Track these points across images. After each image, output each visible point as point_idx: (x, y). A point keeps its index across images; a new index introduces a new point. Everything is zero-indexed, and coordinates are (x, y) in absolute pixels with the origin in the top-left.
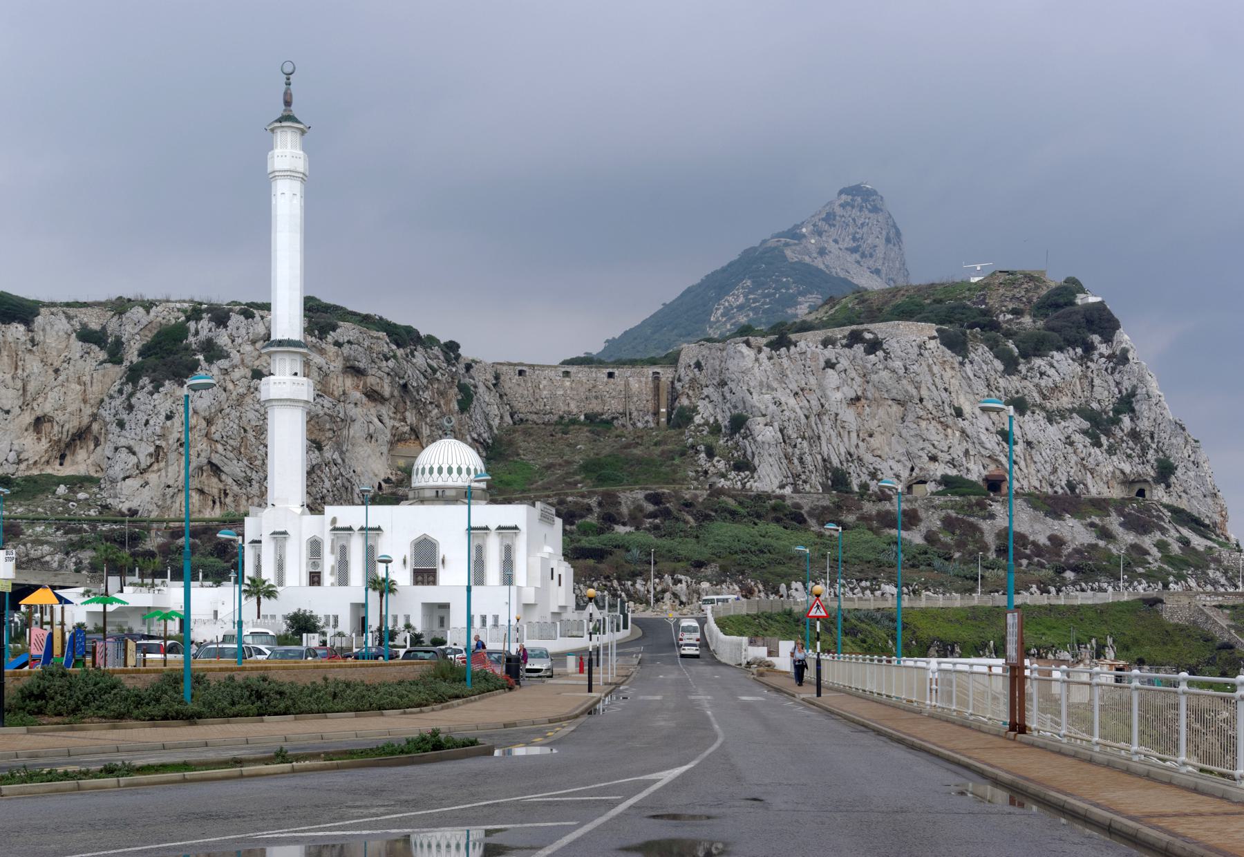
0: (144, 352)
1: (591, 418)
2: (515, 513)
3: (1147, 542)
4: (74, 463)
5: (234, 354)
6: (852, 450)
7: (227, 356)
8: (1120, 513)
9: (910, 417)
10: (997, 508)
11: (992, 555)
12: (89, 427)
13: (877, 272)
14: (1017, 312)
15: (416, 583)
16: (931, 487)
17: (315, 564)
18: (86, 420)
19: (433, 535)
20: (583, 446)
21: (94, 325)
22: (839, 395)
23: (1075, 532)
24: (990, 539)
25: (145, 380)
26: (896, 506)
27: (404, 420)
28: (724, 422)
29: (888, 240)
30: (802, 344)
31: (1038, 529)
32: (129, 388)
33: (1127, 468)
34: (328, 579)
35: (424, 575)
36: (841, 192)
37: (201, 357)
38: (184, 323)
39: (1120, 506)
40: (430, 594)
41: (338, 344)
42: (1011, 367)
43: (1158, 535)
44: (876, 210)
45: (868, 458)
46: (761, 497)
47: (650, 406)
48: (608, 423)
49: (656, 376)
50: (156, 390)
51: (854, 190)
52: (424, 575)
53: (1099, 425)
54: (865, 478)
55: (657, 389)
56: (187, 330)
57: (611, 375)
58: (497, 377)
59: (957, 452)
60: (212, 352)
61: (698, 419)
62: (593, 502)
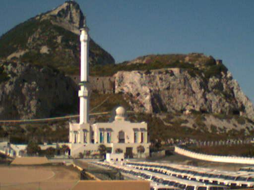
3: (243, 127)
9: (181, 94)
10: (206, 117)
16: (187, 112)
30: (153, 74)
35: (121, 140)
38: (3, 66)
52: (121, 140)
55: (111, 82)
56: (3, 69)
57: (98, 79)
59: (194, 103)
60: (14, 75)
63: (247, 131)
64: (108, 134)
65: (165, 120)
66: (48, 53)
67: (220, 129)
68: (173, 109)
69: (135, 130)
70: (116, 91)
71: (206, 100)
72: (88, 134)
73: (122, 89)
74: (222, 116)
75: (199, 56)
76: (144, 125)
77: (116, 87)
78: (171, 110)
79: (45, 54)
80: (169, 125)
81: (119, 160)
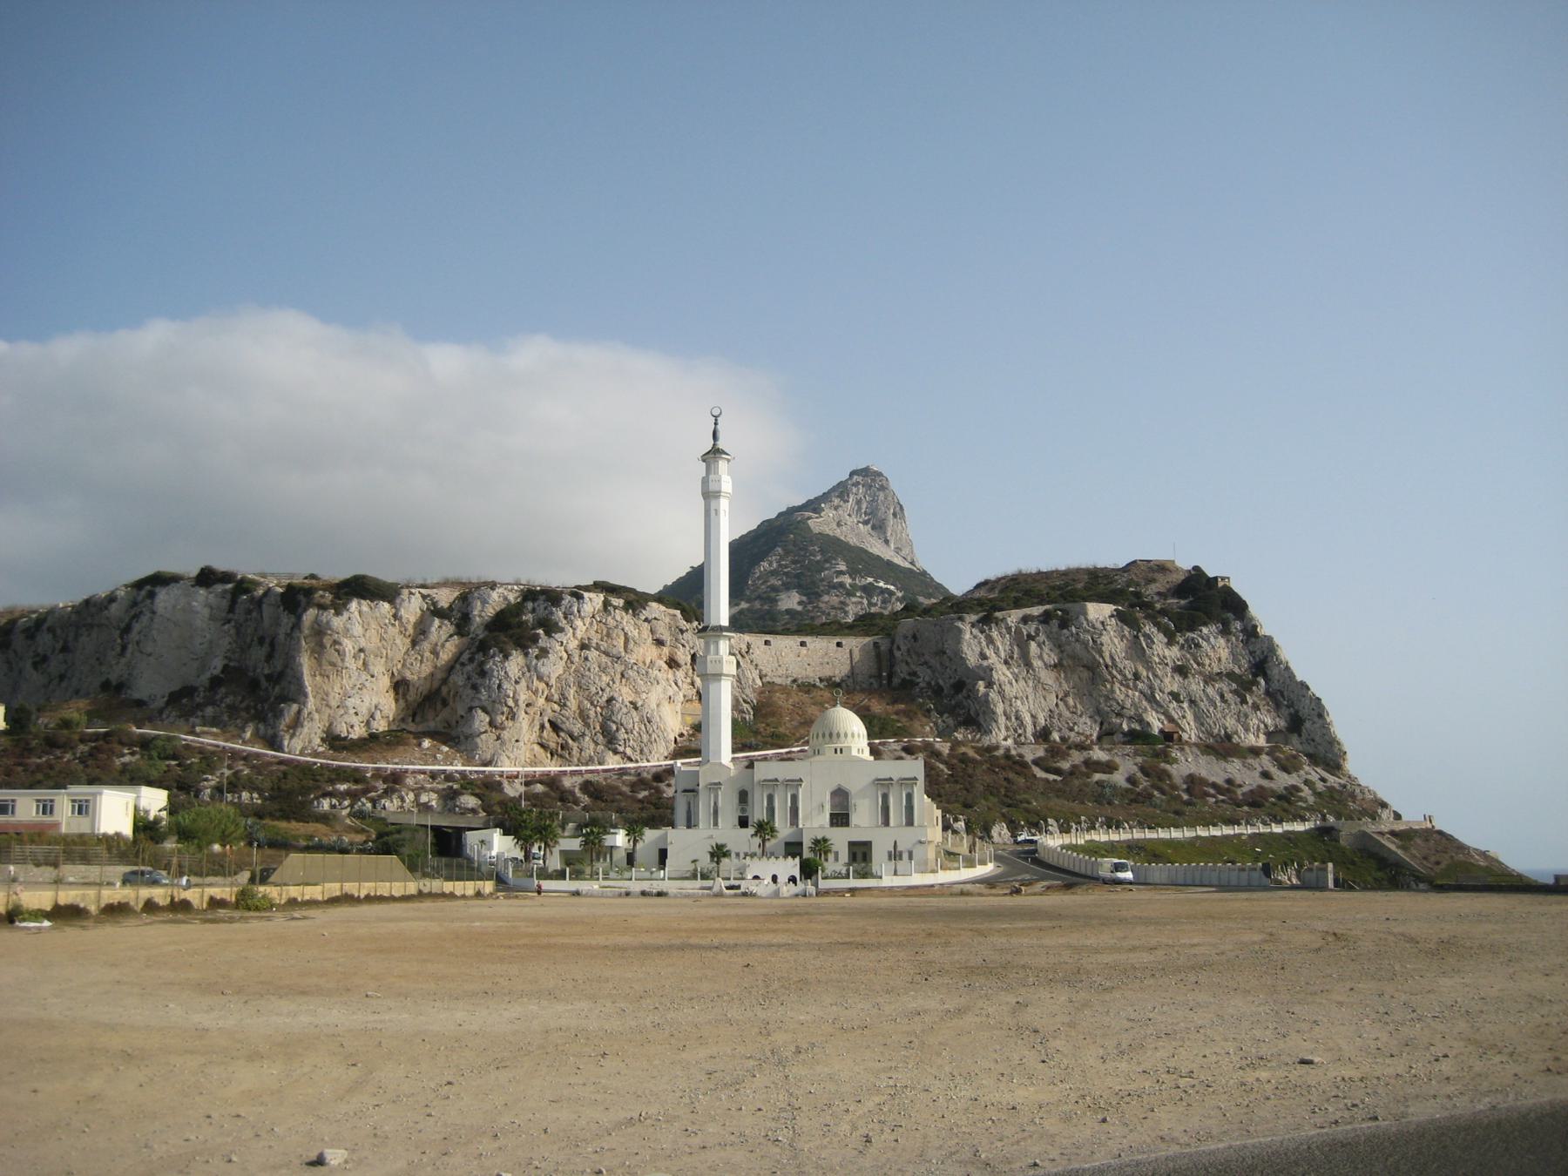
4: (424, 720)
5: (568, 628)
6: (1053, 707)
7: (562, 630)
12: (439, 690)
13: (887, 542)
15: (832, 824)
16: (1118, 737)
17: (743, 810)
18: (436, 684)
19: (846, 786)
27: (693, 684)
29: (895, 515)
31: (1213, 770)
32: (479, 657)
33: (1269, 721)
35: (840, 819)
36: (852, 474)
37: (541, 631)
41: (646, 620)
44: (883, 488)
47: (874, 671)
50: (506, 657)
51: (865, 472)
52: (840, 819)
53: (1243, 687)
55: (878, 656)
57: (839, 645)
58: (749, 646)
63: (1306, 792)
65: (1036, 762)
66: (799, 608)
67: (1214, 785)
69: (884, 783)
70: (896, 681)
71: (1175, 696)
73: (914, 674)
74: (1222, 747)
75: (1162, 568)
76: (914, 767)
77: (897, 669)
78: (1067, 733)
79: (788, 611)
80: (1052, 777)
81: (782, 879)
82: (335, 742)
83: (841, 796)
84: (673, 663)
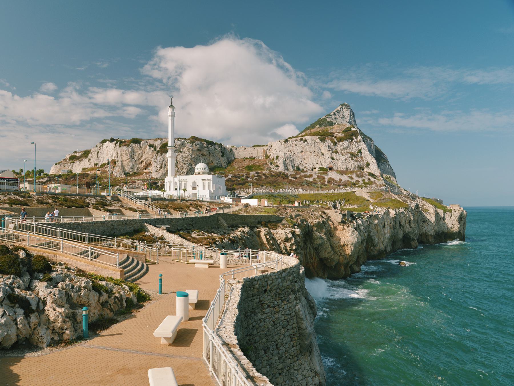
0: (160, 148)
1: (251, 158)
2: (210, 176)
8: (356, 174)
11: (326, 183)
14: (339, 133)
16: (317, 169)
20: (247, 163)
21: (152, 144)
22: (298, 151)
23: (345, 178)
24: (326, 180)
25: (159, 153)
26: (308, 173)
28: (275, 157)
34: (178, 189)
39: (356, 172)
40: (195, 192)
41: (196, 145)
42: (335, 144)
43: (363, 178)
45: (304, 164)
46: (280, 172)
48: (254, 158)
49: (263, 149)
52: (194, 188)
54: (303, 168)
61: (270, 157)
62: (244, 174)
64: (185, 184)
68: (305, 167)
71: (333, 159)
72: (172, 184)
82: (127, 174)
83: (194, 183)
84: (203, 155)
